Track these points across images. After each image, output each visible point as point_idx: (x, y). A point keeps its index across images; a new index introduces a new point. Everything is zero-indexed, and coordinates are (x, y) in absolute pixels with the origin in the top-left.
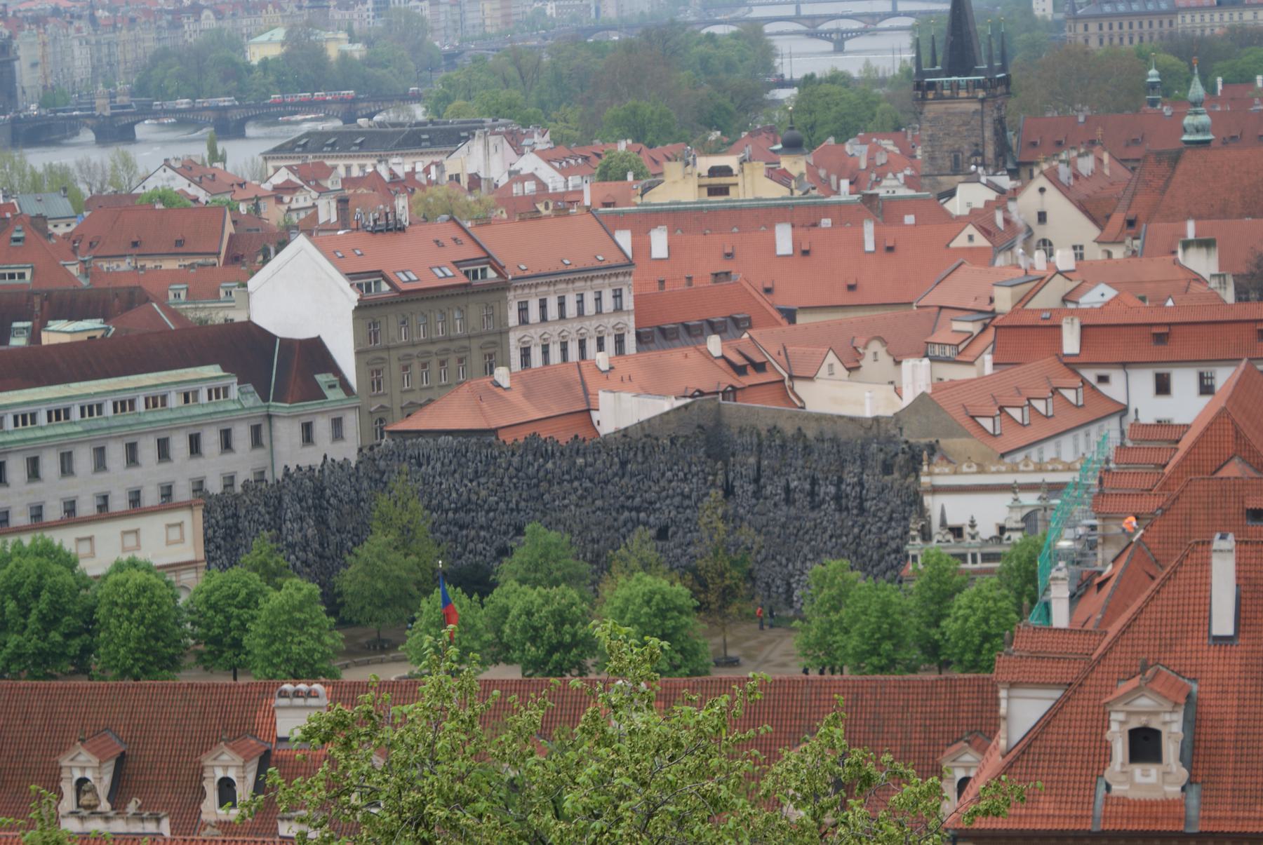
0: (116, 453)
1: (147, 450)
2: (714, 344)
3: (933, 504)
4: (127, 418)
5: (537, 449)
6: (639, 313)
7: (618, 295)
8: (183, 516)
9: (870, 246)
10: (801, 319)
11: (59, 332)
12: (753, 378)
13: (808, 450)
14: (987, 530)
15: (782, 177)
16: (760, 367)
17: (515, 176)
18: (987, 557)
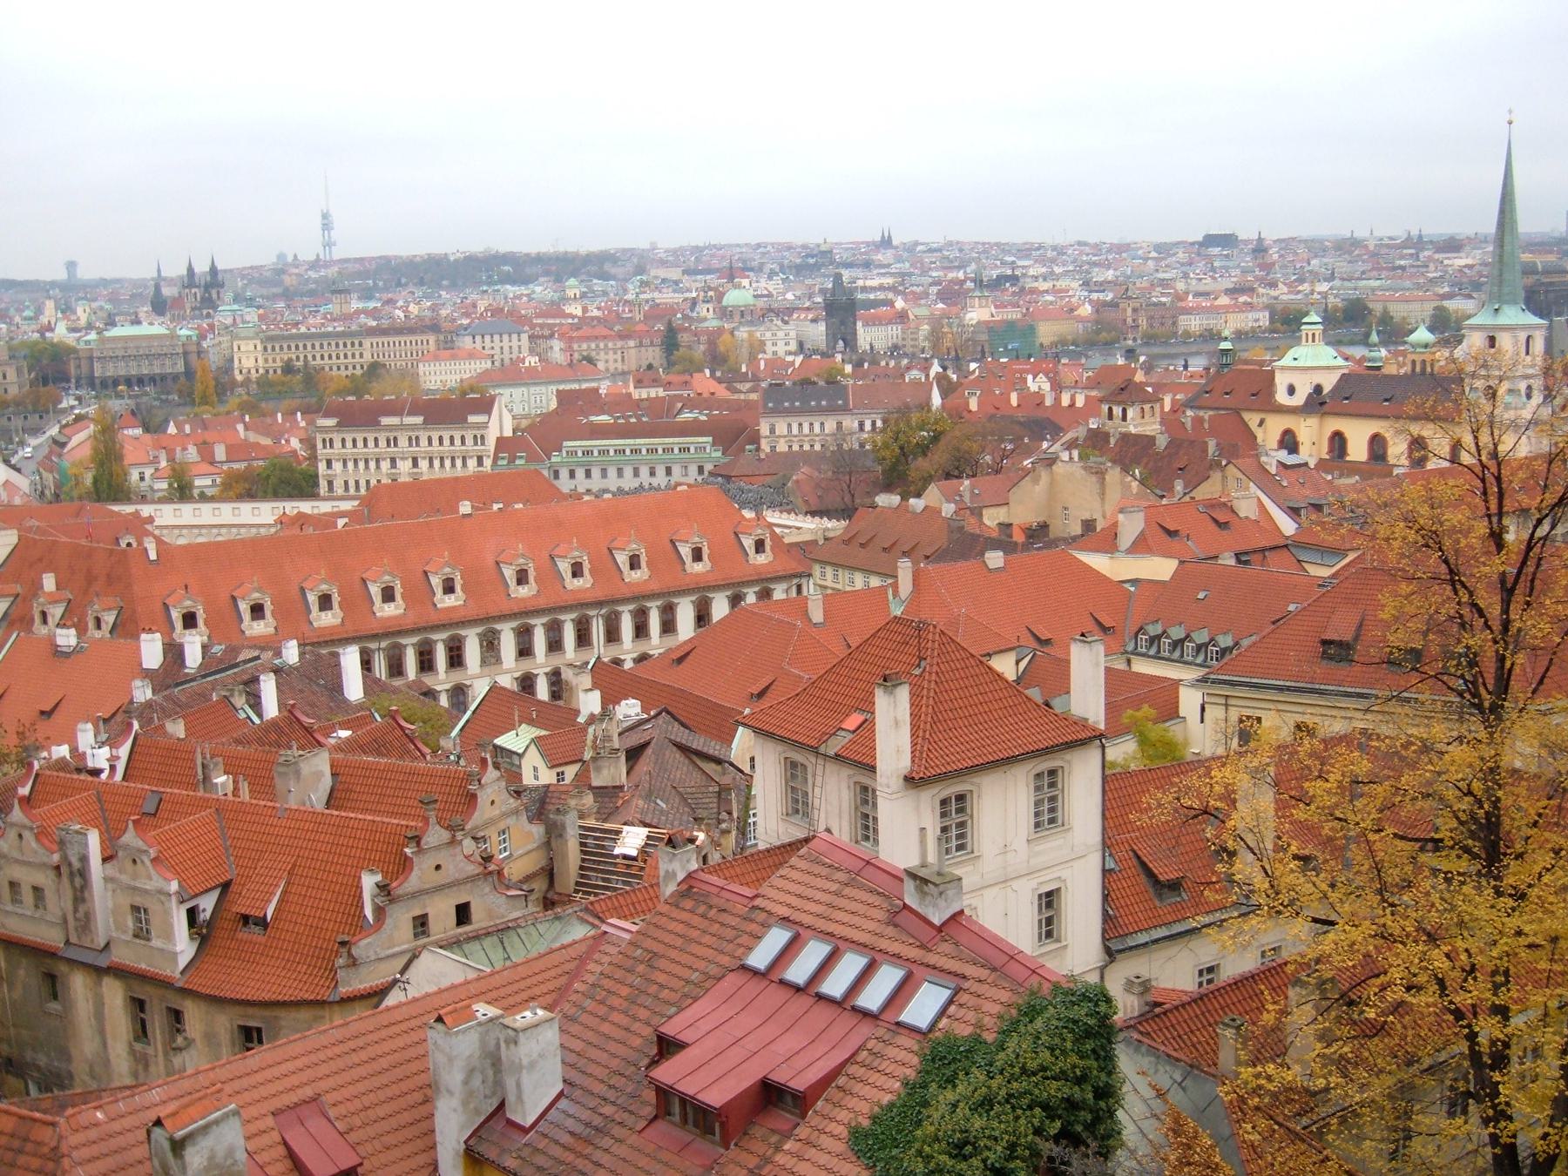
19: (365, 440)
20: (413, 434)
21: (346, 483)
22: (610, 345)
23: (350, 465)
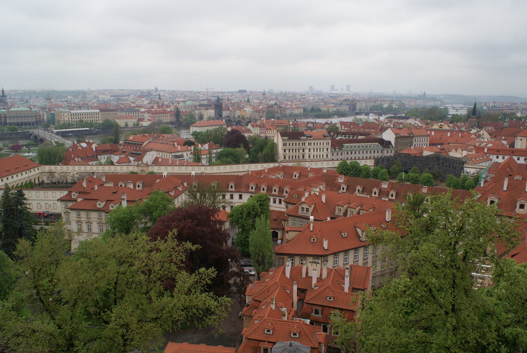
0: (365, 152)
1: (369, 152)
2: (439, 146)
3: (465, 169)
4: (367, 148)
5: (415, 157)
6: (430, 141)
7: (427, 139)
8: (372, 160)
9: (460, 136)
10: (450, 144)
11: (360, 137)
12: (443, 151)
13: (450, 160)
14: (472, 173)
15: (449, 126)
16: (444, 150)
17: (415, 123)
18: (471, 176)
19: (296, 144)
20: (310, 142)
21: (289, 156)
22: (164, 115)
23: (291, 151)
